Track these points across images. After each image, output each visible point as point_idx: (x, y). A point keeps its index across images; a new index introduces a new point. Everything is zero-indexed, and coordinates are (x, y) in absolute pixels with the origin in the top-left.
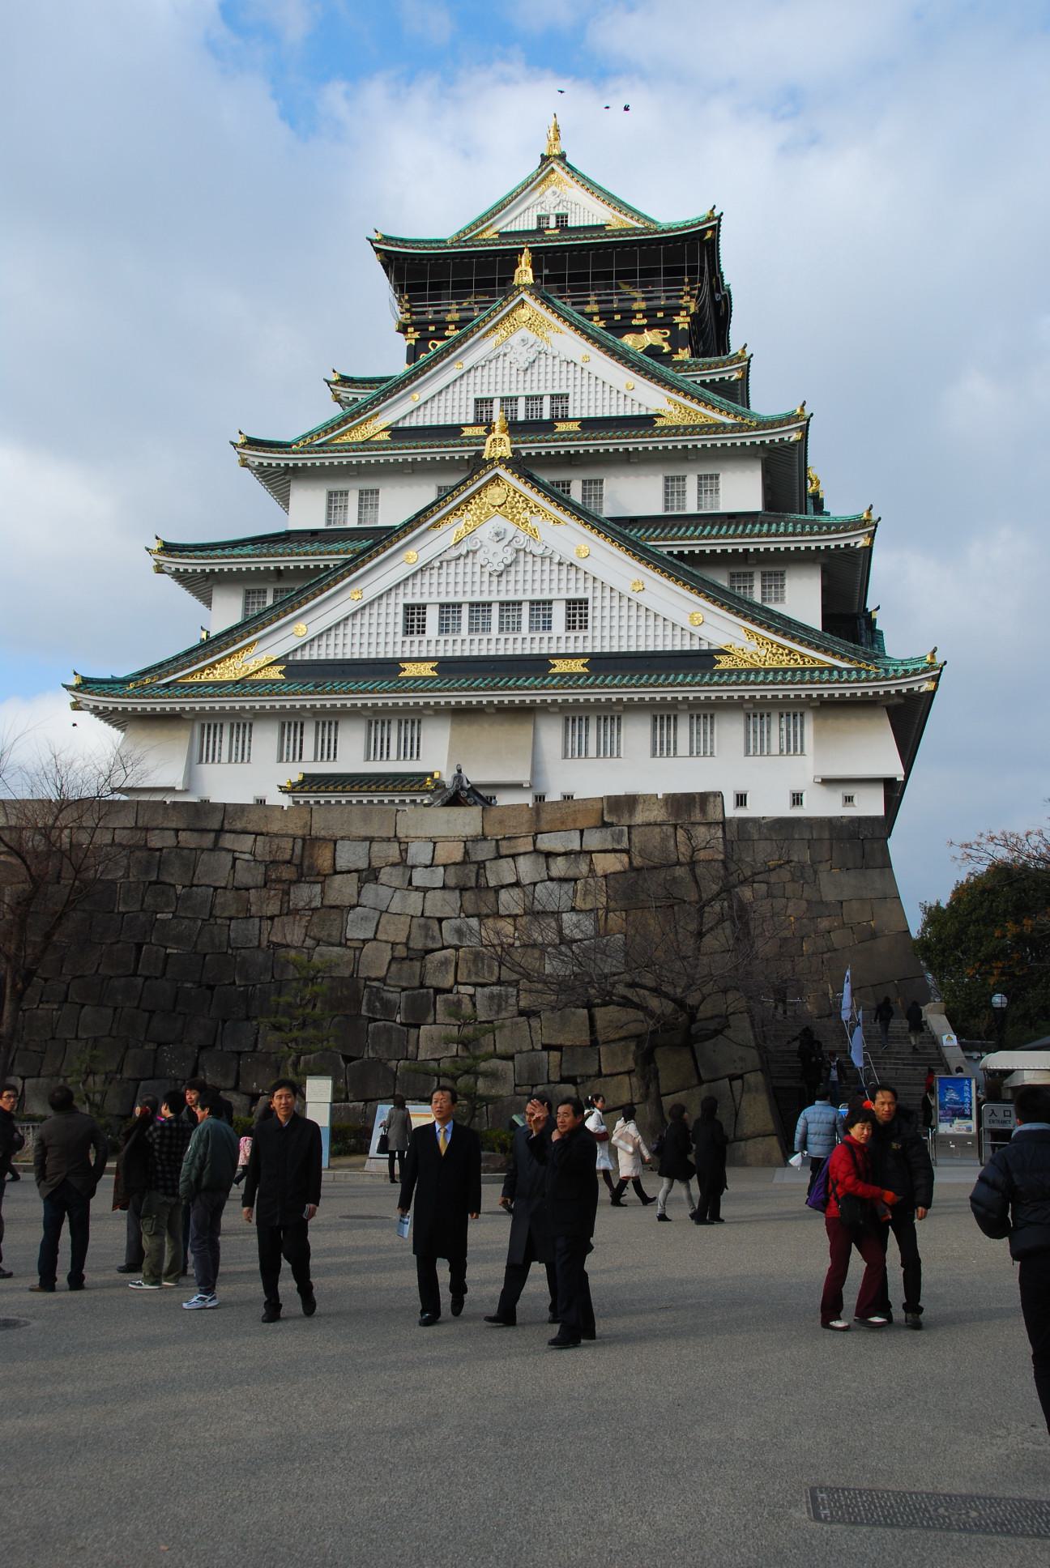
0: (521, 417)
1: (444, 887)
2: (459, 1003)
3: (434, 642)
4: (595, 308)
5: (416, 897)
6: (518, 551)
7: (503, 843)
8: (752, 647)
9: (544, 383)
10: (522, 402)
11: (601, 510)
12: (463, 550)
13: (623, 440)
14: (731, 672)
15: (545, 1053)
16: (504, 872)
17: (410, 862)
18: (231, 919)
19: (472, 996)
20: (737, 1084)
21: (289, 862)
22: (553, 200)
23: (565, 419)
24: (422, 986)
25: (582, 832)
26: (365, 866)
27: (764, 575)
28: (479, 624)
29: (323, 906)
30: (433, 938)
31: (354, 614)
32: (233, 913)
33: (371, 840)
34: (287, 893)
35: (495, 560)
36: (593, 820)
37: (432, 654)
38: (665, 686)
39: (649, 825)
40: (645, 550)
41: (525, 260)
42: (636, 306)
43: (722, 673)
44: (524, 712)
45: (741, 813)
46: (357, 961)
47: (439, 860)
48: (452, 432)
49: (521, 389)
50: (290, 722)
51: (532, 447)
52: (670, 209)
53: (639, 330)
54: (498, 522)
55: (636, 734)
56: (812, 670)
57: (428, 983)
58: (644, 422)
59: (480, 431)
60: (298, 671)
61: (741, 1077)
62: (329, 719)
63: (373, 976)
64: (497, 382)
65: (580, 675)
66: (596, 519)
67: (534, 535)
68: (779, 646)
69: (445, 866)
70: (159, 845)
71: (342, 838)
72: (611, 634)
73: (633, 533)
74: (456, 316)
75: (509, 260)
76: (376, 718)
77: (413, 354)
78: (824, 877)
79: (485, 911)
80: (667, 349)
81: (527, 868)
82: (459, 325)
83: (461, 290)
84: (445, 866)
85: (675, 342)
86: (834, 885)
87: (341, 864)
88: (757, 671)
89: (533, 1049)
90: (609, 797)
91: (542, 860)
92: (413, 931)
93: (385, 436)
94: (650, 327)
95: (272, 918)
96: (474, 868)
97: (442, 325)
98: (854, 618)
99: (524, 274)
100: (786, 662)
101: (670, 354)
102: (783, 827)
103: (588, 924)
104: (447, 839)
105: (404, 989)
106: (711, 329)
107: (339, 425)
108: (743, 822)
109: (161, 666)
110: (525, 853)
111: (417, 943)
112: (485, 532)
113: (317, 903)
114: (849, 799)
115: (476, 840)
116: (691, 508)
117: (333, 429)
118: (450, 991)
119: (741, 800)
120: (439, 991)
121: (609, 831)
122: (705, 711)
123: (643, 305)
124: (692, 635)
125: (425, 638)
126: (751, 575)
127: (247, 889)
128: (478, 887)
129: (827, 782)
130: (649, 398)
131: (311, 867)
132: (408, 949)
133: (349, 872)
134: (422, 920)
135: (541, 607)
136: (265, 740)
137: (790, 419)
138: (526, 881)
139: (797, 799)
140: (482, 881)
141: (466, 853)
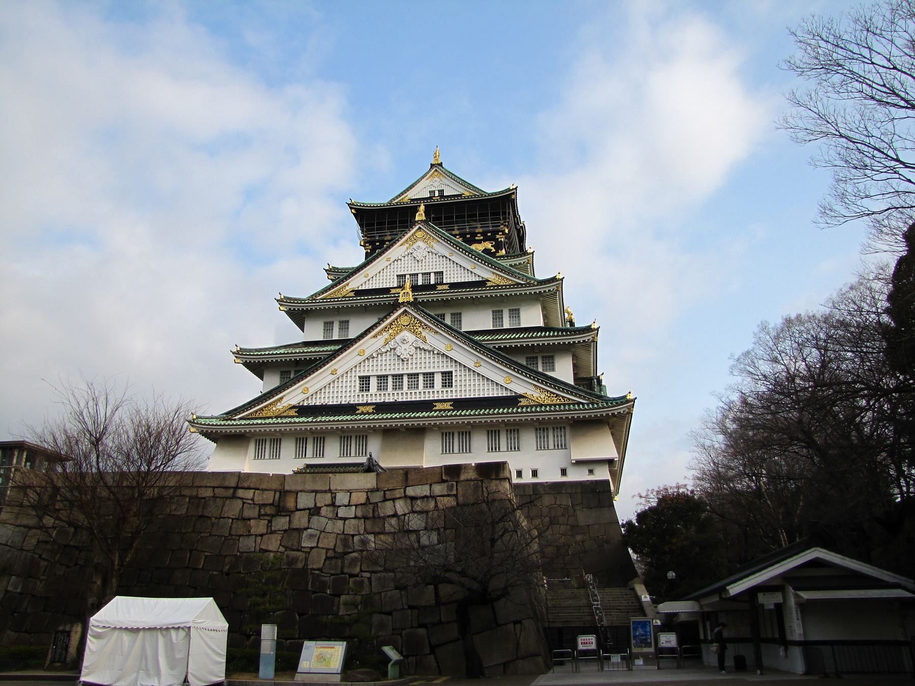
0: (420, 283)
1: (356, 517)
2: (362, 581)
3: (375, 395)
5: (340, 523)
6: (416, 348)
7: (387, 493)
9: (431, 265)
10: (420, 276)
11: (460, 328)
12: (387, 348)
13: (471, 295)
14: (527, 407)
15: (409, 611)
16: (387, 509)
17: (337, 503)
18: (240, 536)
19: (369, 579)
20: (518, 626)
21: (272, 504)
22: (436, 184)
23: (442, 284)
24: (342, 573)
25: (431, 485)
26: (313, 506)
27: (543, 357)
28: (398, 386)
29: (290, 529)
30: (349, 547)
31: (334, 382)
32: (241, 533)
33: (316, 492)
34: (270, 521)
35: (405, 353)
36: (436, 479)
37: (374, 401)
38: (497, 417)
39: (468, 480)
40: (481, 346)
41: (422, 208)
42: (477, 231)
43: (522, 407)
45: (535, 480)
46: (306, 559)
47: (352, 503)
48: (386, 291)
50: (301, 438)
51: (424, 297)
52: (491, 186)
53: (479, 242)
54: (406, 334)
56: (569, 404)
57: (346, 570)
58: (482, 283)
59: (398, 290)
60: (303, 410)
61: (520, 622)
62: (320, 437)
63: (314, 567)
64: (408, 268)
65: (449, 410)
66: (460, 333)
67: (424, 340)
68: (551, 393)
69: (356, 506)
70: (204, 495)
71: (301, 491)
72: (467, 387)
73: (477, 338)
74: (389, 238)
75: (415, 210)
76: (344, 436)
77: (367, 255)
78: (578, 513)
79: (377, 530)
80: (494, 250)
81: (401, 507)
82: (389, 241)
83: (392, 225)
84: (356, 506)
85: (498, 246)
86: (584, 517)
87: (300, 506)
88: (541, 405)
89: (403, 609)
90: (445, 466)
91: (409, 501)
92: (338, 542)
93: (352, 294)
94: (485, 240)
95: (262, 535)
96: (371, 507)
97: (383, 242)
98: (591, 379)
99: (420, 216)
100: (555, 401)
101: (494, 253)
102: (556, 488)
103: (434, 537)
104: (357, 490)
105: (332, 575)
106: (516, 242)
107: (330, 289)
108: (535, 485)
109: (236, 409)
110: (400, 498)
111: (340, 549)
112: (398, 338)
113: (286, 527)
114: (591, 472)
115: (372, 491)
116: (506, 325)
117: (326, 291)
118: (357, 576)
119: (535, 473)
120: (351, 576)
121: (446, 484)
123: (481, 230)
124: (506, 389)
125: (369, 394)
126: (537, 358)
127: (249, 519)
128: (374, 517)
130: (483, 273)
131: (284, 507)
132: (335, 552)
133: (304, 510)
134: (343, 536)
135: (429, 376)
136: (288, 448)
137: (554, 279)
138: (400, 512)
139: (564, 472)
140: (376, 514)
141: (368, 498)
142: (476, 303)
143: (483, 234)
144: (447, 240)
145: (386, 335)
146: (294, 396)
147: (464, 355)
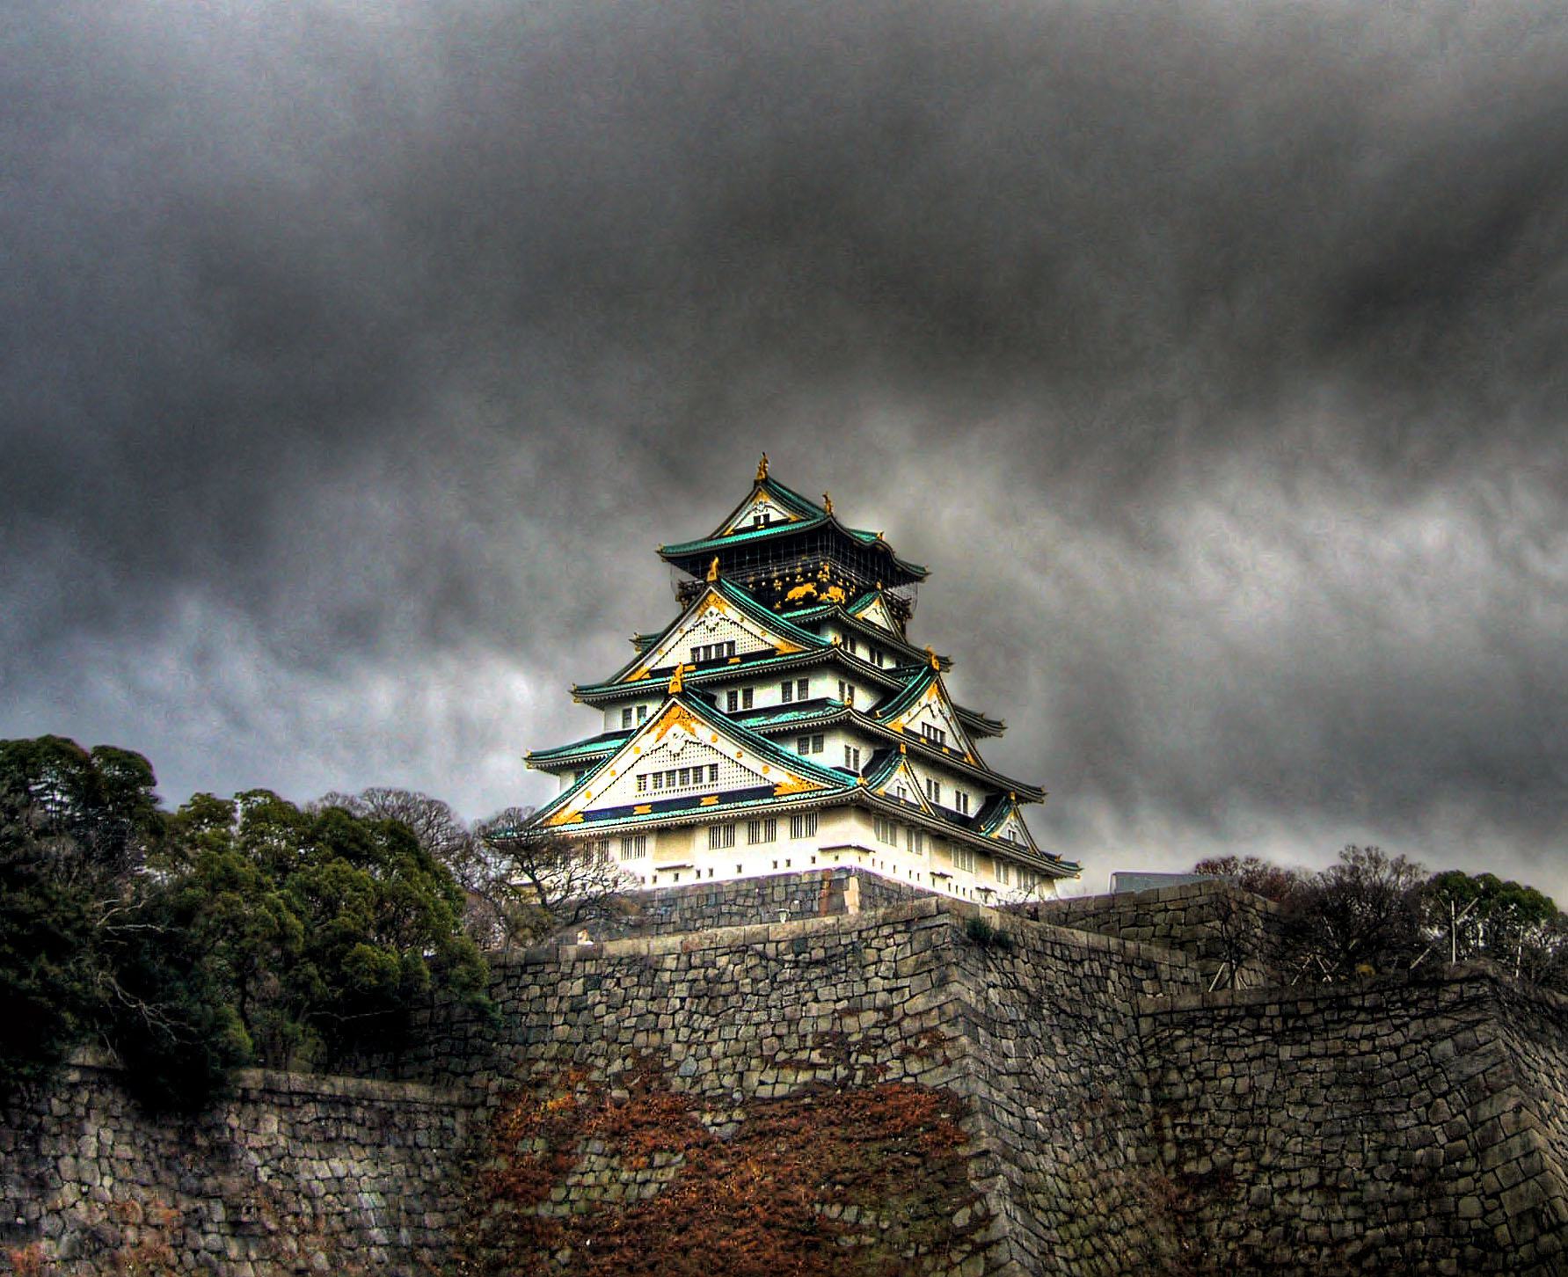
4: (775, 574)
8: (790, 781)
44: (687, 829)
49: (711, 641)
53: (800, 584)
54: (677, 728)
55: (741, 835)
58: (771, 653)
60: (588, 816)
67: (693, 734)
94: (807, 581)
108: (788, 876)
112: (670, 733)
116: (795, 699)
122: (771, 819)
129: (823, 850)
135: (698, 769)
142: (765, 678)
143: (803, 574)
144: (735, 602)
145: (657, 730)
146: (580, 803)
147: (729, 747)
